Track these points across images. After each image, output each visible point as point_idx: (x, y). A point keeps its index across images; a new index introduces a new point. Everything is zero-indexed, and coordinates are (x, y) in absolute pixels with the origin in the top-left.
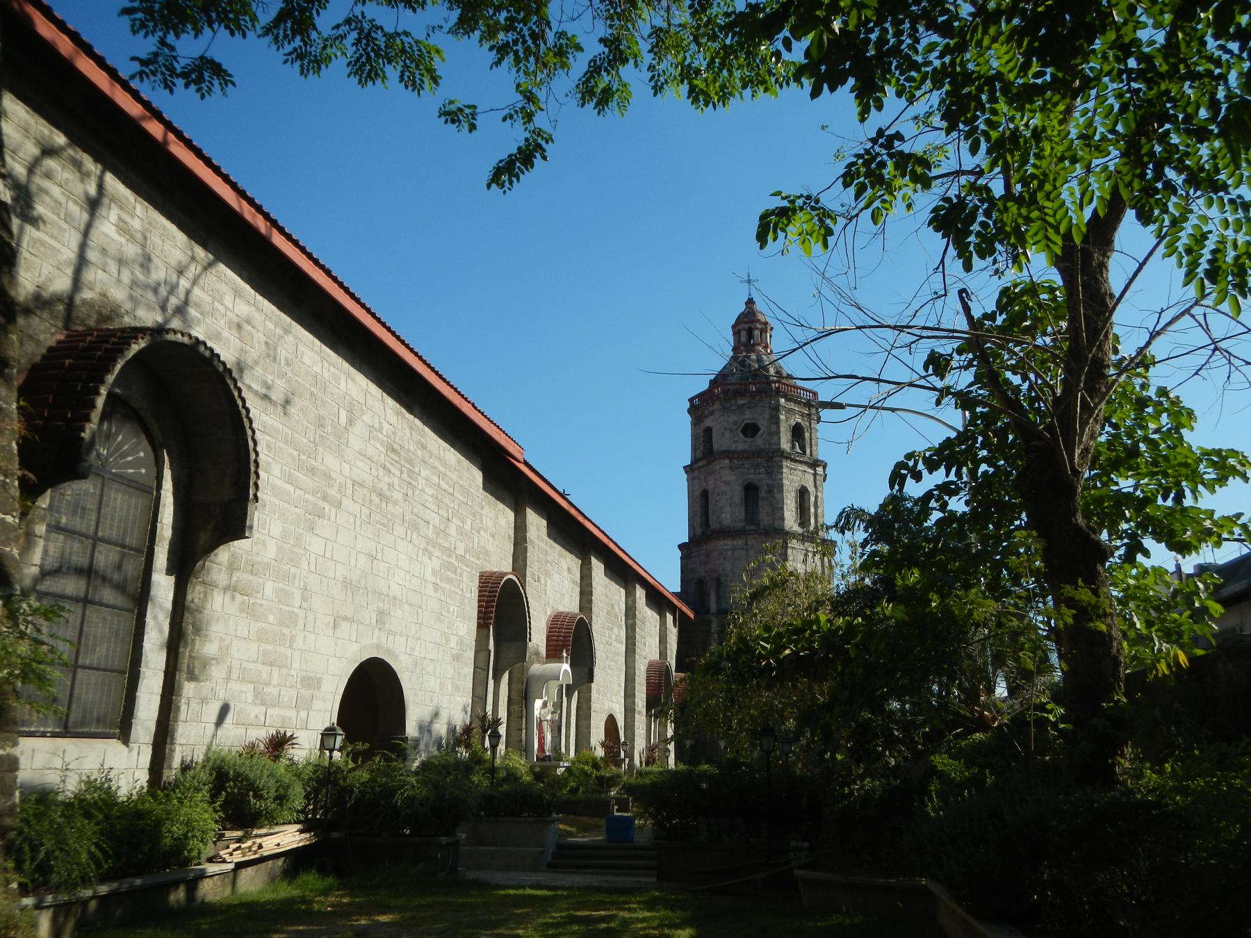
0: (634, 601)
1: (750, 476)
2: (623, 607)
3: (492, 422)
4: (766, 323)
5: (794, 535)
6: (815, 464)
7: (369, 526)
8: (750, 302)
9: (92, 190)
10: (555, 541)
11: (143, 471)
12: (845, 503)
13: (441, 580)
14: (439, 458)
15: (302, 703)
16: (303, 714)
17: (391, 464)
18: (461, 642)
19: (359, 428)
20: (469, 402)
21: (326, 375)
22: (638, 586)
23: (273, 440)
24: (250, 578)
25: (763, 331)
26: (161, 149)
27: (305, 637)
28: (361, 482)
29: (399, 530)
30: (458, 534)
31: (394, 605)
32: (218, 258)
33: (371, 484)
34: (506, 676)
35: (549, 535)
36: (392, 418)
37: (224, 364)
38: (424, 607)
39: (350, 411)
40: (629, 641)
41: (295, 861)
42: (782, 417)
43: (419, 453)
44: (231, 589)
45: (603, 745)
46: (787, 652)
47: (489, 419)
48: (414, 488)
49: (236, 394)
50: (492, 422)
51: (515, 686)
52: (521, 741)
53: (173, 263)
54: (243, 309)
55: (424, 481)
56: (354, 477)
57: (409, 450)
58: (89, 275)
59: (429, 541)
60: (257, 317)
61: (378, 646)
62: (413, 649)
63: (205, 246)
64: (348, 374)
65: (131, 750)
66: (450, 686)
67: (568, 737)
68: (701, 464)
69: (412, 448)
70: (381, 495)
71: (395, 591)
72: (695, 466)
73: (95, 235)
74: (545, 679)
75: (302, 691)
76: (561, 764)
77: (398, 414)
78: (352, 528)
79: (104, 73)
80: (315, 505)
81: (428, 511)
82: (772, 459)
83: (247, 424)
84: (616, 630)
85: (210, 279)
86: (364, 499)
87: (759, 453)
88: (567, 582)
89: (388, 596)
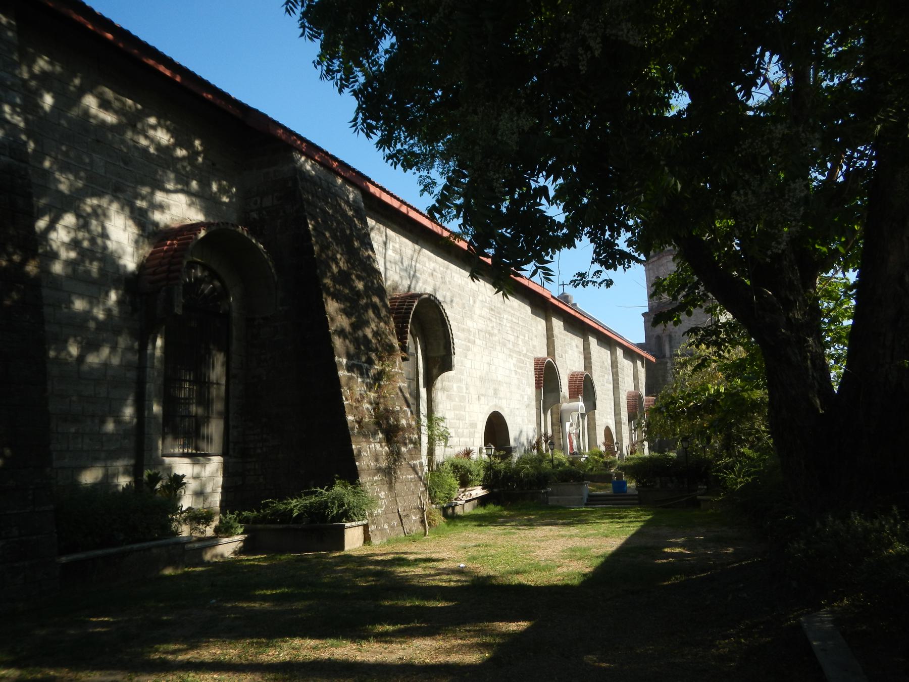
0: (616, 358)
15: (471, 435)
16: (472, 439)
18: (529, 398)
19: (478, 304)
21: (463, 283)
22: (618, 348)
24: (448, 384)
29: (498, 348)
32: (422, 247)
35: (565, 329)
37: (439, 301)
39: (474, 297)
40: (615, 382)
41: (482, 501)
45: (604, 444)
46: (692, 404)
49: (443, 311)
51: (554, 416)
53: (409, 256)
54: (432, 265)
59: (510, 350)
61: (496, 406)
62: (509, 405)
63: (417, 244)
67: (584, 441)
69: (499, 305)
70: (489, 333)
71: (500, 378)
73: (387, 256)
74: (570, 411)
80: (466, 345)
83: (448, 323)
84: (606, 377)
85: (421, 258)
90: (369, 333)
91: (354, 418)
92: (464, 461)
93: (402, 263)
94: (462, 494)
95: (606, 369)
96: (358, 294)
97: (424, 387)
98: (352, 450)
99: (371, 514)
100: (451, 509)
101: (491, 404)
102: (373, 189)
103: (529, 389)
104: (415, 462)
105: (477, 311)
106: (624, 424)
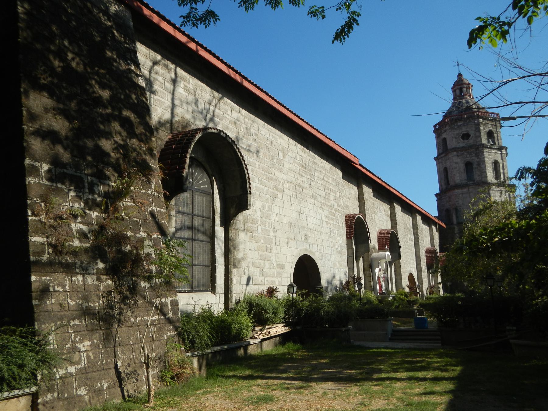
0: (416, 222)
1: (467, 158)
3: (343, 149)
4: (469, 84)
5: (493, 184)
6: (501, 148)
7: (297, 200)
8: (460, 75)
9: (173, 76)
10: (377, 198)
11: (206, 186)
12: (520, 165)
14: (322, 167)
16: (279, 279)
18: (340, 246)
19: (287, 159)
20: (332, 141)
21: (271, 138)
22: (417, 215)
23: (254, 168)
24: (252, 225)
25: (468, 88)
26: (195, 54)
29: (309, 200)
30: (334, 199)
34: (361, 259)
35: (374, 196)
36: (300, 152)
37: (231, 139)
38: (323, 232)
39: (283, 152)
41: (284, 338)
42: (482, 128)
43: (314, 166)
44: (245, 230)
45: (408, 286)
46: (497, 239)
47: (342, 148)
48: (313, 181)
49: (237, 151)
50: (343, 149)
51: (366, 263)
52: (371, 286)
53: (206, 100)
54: (235, 115)
56: (288, 180)
57: (309, 165)
58: (177, 110)
59: (322, 203)
60: (241, 118)
61: (306, 250)
62: (320, 250)
65: (216, 296)
67: (392, 284)
68: (442, 156)
69: (310, 164)
70: (300, 186)
71: (310, 226)
72: (439, 157)
73: (176, 94)
74: (379, 259)
76: (390, 295)
77: (303, 150)
78: (290, 201)
79: (171, 27)
80: (273, 193)
82: (479, 149)
83: (243, 163)
84: (409, 235)
85: (221, 104)
86: (293, 188)
87: (471, 147)
88: (384, 216)
90: (106, 145)
91: (45, 239)
92: (266, 302)
93: (196, 102)
94: (259, 333)
96: (98, 101)
97: (221, 226)
98: (30, 283)
99: (52, 377)
100: (242, 349)
101: (301, 248)
102: (146, 12)
103: (341, 238)
104: (163, 300)
105: (287, 165)
106: (424, 272)
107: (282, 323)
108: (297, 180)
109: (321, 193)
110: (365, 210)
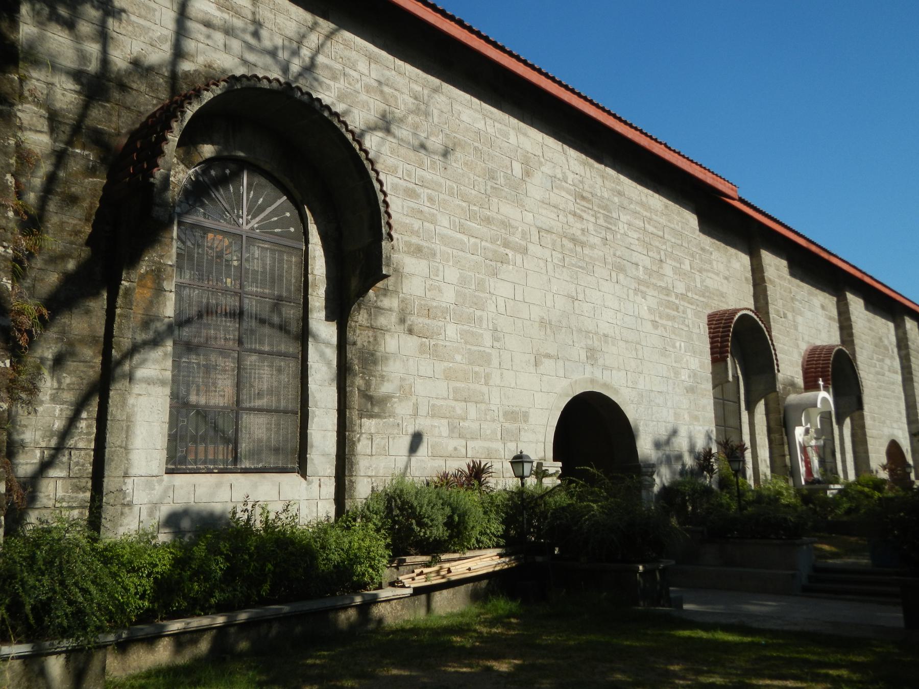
0: (905, 333)
2: (893, 339)
3: (692, 161)
7: (565, 270)
11: (292, 230)
13: (660, 317)
14: (642, 204)
17: (582, 210)
18: (694, 374)
19: (537, 178)
20: (661, 143)
21: (490, 130)
23: (434, 193)
27: (502, 374)
28: (548, 228)
30: (675, 273)
31: (606, 342)
33: (560, 230)
34: (760, 408)
35: (793, 274)
36: (579, 168)
38: (644, 343)
39: (526, 163)
47: (688, 159)
48: (614, 233)
50: (692, 161)
51: (772, 416)
55: (626, 226)
56: (540, 225)
57: (602, 197)
60: (400, 81)
61: (592, 381)
64: (519, 130)
65: (309, 483)
66: (686, 416)
69: (606, 195)
70: (574, 240)
71: (604, 328)
75: (507, 425)
76: (832, 486)
77: (584, 164)
78: (544, 271)
80: (495, 251)
81: (635, 254)
84: (888, 361)
86: (554, 244)
89: (596, 333)
95: (886, 348)
107: (494, 547)
108: (566, 226)
109: (636, 257)
110: (767, 303)
